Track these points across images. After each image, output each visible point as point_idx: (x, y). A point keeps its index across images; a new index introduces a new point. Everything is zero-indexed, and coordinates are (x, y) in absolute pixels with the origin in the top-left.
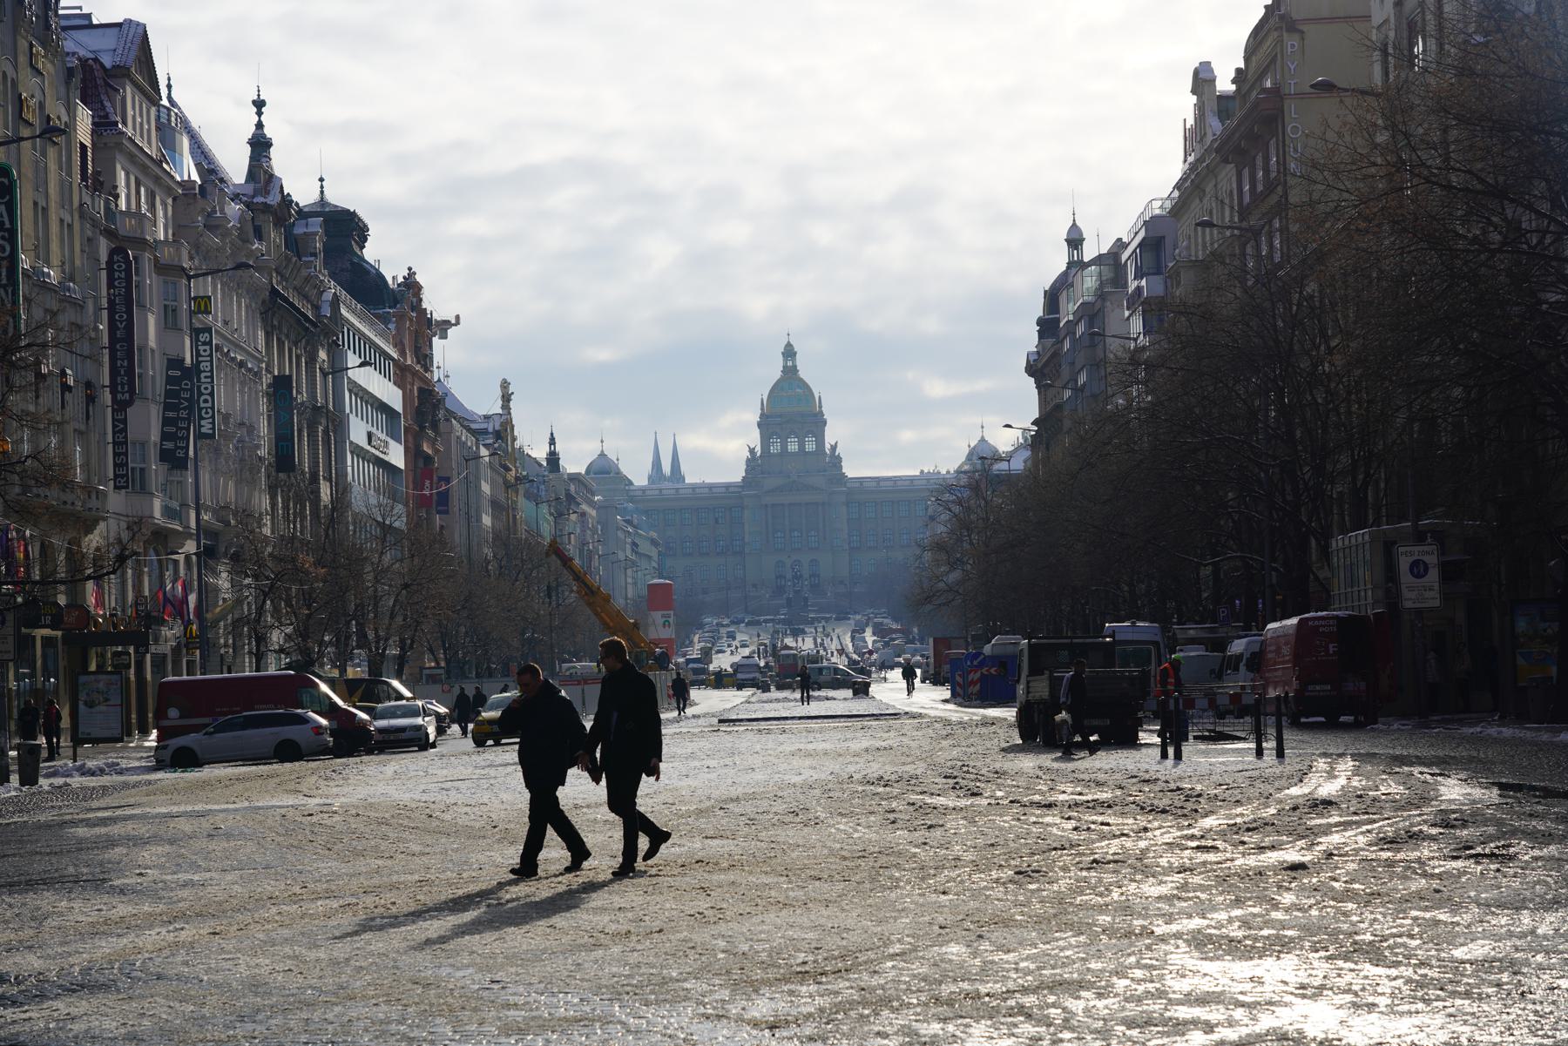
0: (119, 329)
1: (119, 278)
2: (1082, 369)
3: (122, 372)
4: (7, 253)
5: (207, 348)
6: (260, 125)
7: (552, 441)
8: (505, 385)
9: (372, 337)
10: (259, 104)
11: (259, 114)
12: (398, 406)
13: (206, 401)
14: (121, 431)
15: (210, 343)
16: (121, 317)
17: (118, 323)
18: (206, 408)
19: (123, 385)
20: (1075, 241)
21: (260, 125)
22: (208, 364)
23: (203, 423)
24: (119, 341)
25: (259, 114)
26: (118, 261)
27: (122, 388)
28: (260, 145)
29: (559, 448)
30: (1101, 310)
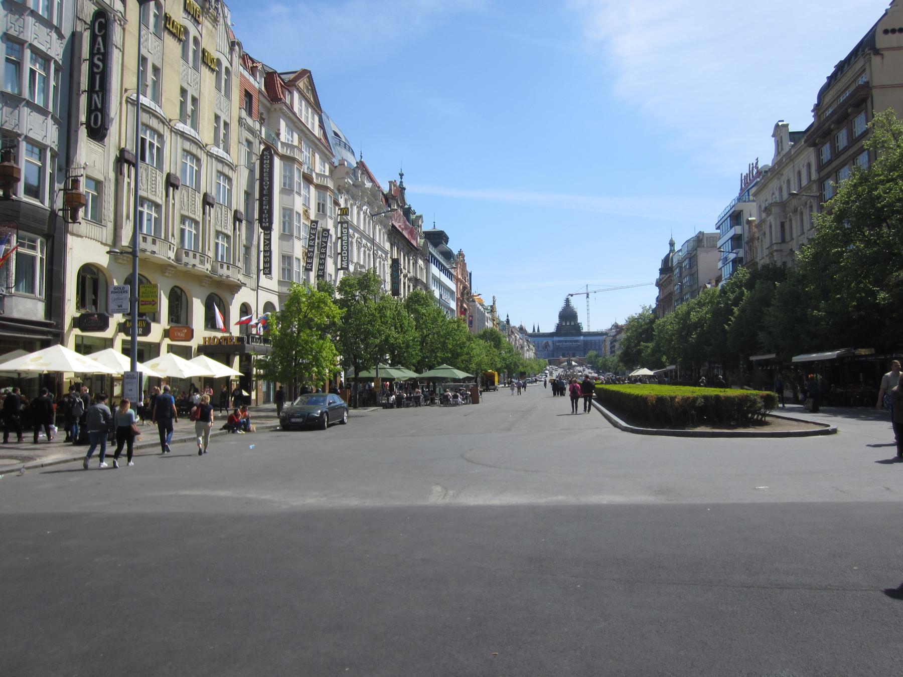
0: (264, 189)
1: (266, 163)
2: (686, 277)
3: (266, 212)
4: (100, 70)
5: (346, 230)
7: (508, 316)
8: (494, 297)
9: (441, 261)
10: (401, 175)
11: (401, 178)
12: (455, 290)
13: (345, 253)
14: (267, 245)
16: (266, 183)
17: (265, 187)
18: (345, 256)
19: (265, 218)
20: (672, 244)
22: (346, 237)
23: (343, 263)
24: (266, 195)
25: (401, 178)
26: (266, 155)
27: (266, 220)
29: (509, 318)
30: (696, 256)
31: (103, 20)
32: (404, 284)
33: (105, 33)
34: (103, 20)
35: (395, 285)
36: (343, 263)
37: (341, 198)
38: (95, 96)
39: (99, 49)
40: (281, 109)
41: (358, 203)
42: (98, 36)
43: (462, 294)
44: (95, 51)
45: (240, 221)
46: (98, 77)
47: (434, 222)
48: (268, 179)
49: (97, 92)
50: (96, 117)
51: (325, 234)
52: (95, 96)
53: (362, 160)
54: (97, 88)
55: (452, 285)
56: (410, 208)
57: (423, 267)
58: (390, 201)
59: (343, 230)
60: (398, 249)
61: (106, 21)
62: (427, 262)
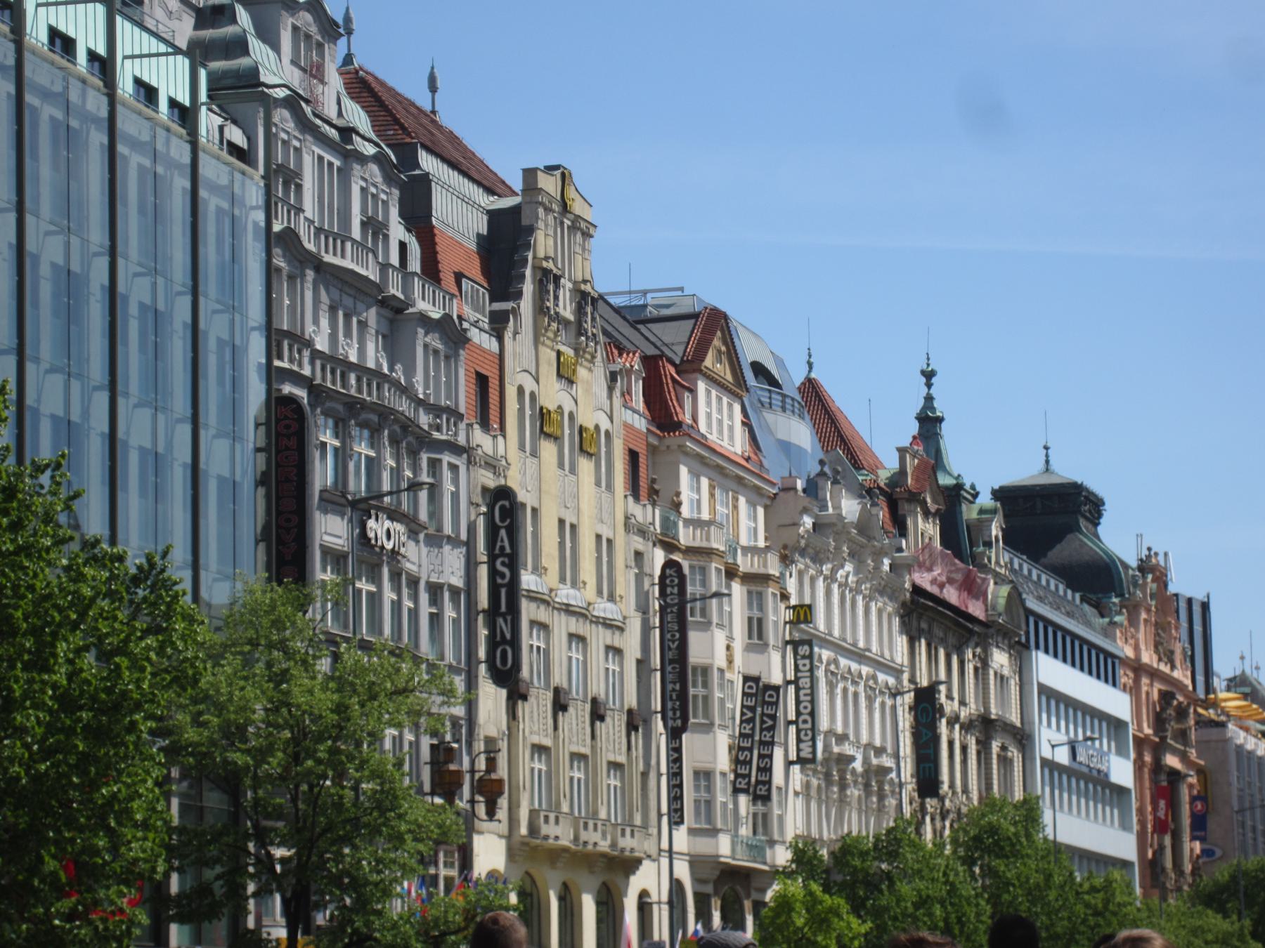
1: (672, 594)
4: (507, 580)
5: (807, 662)
6: (929, 399)
10: (929, 375)
11: (929, 385)
13: (805, 722)
15: (810, 656)
18: (806, 730)
21: (929, 399)
22: (808, 680)
23: (802, 746)
25: (929, 385)
26: (671, 576)
28: (929, 423)
31: (507, 503)
32: (951, 744)
33: (511, 524)
34: (507, 503)
35: (927, 765)
36: (802, 746)
37: (791, 576)
38: (500, 621)
39: (502, 548)
40: (681, 447)
41: (826, 568)
42: (500, 528)
43: (1159, 722)
44: (497, 551)
45: (636, 729)
46: (503, 591)
47: (1046, 448)
48: (676, 628)
49: (504, 615)
50: (504, 653)
51: (771, 696)
52: (500, 621)
53: (813, 375)
54: (503, 609)
55: (1115, 702)
56: (959, 487)
57: (1006, 672)
58: (904, 507)
59: (801, 662)
60: (929, 645)
61: (511, 504)
62: (1020, 651)
